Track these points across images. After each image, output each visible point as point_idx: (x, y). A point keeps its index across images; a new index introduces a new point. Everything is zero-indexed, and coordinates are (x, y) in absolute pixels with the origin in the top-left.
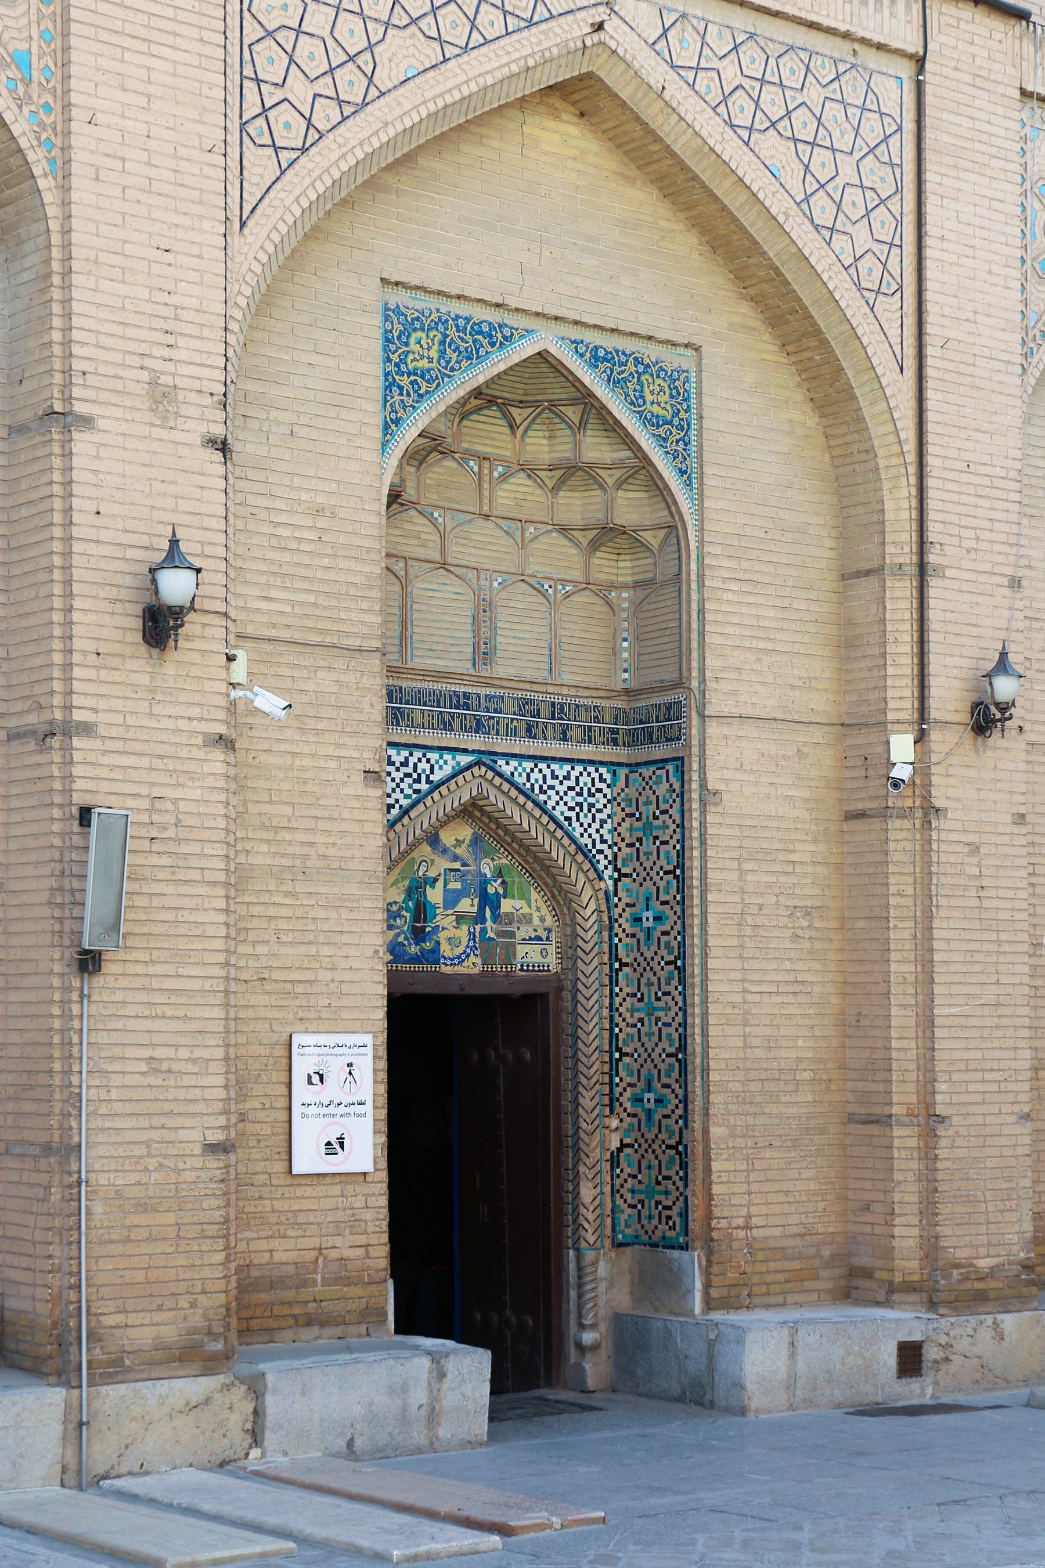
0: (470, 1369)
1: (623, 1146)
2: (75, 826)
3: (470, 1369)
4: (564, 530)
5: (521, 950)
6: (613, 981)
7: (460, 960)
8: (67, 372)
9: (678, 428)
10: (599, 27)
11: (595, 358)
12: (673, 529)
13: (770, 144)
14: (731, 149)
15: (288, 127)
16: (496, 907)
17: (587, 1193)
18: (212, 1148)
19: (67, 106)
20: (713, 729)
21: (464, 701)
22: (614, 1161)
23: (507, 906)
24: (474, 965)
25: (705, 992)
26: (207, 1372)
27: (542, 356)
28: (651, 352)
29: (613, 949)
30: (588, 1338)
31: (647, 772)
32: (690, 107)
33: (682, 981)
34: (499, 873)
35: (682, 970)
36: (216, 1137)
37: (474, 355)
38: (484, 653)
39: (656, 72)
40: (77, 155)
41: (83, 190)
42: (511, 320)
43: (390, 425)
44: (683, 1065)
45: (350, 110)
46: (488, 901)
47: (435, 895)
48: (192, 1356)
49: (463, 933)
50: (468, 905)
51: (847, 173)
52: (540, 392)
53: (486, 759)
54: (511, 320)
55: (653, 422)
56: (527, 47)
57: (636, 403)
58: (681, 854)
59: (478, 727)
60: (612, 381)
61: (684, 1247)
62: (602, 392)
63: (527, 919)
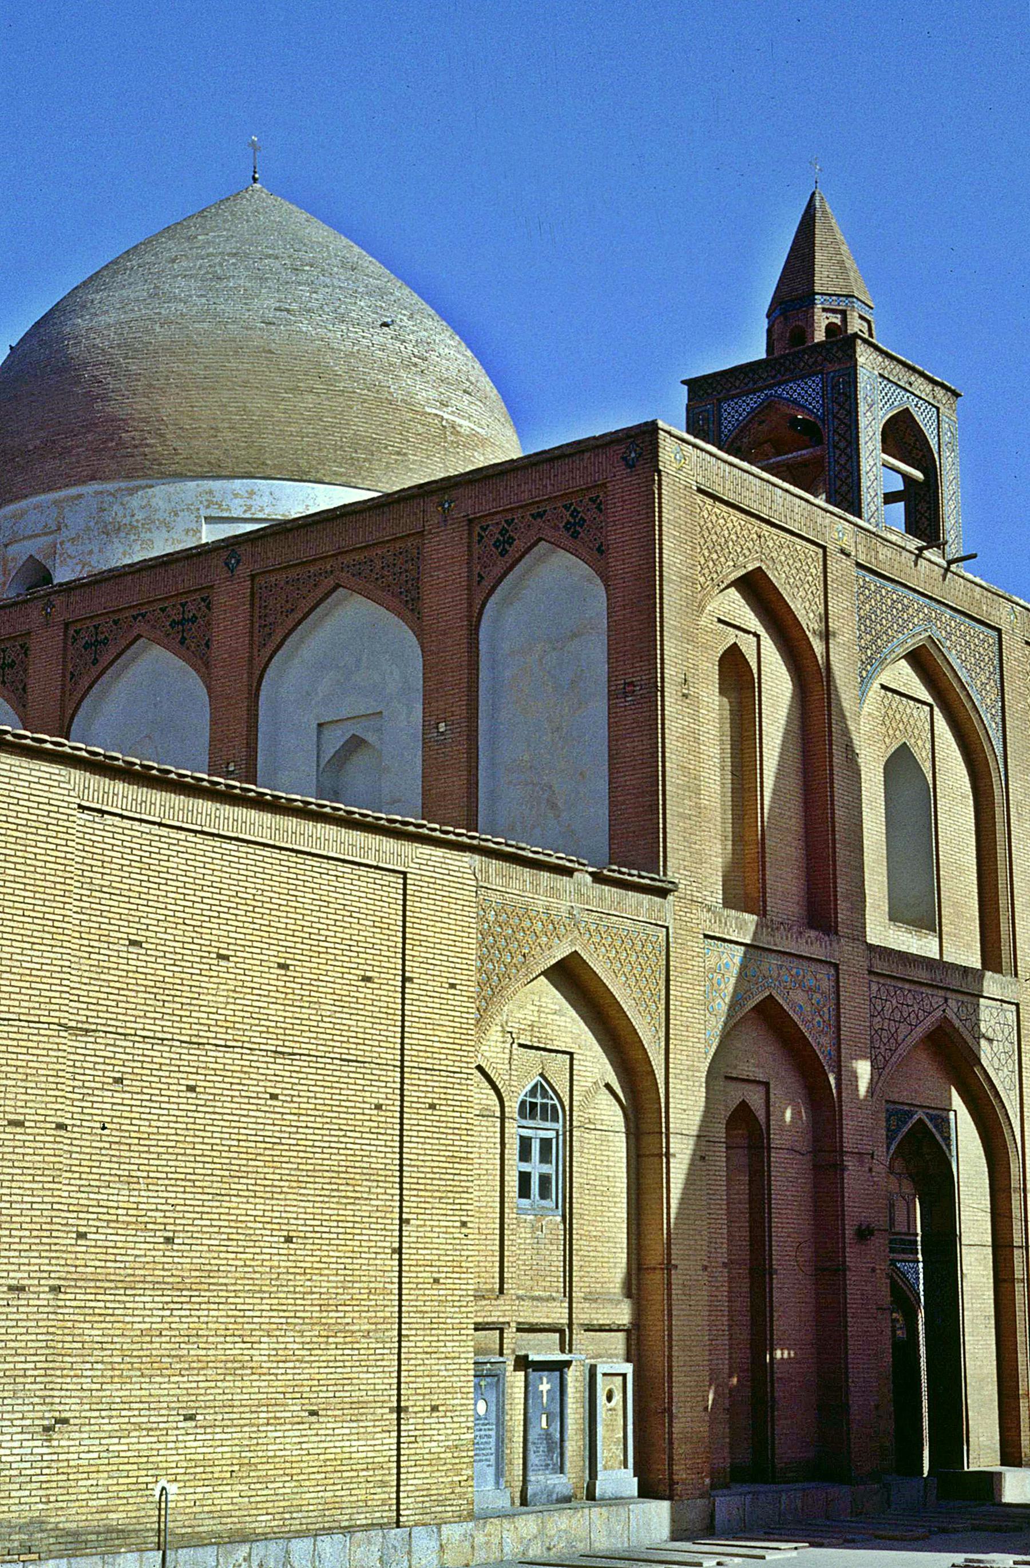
11: (932, 1118)
39: (957, 1023)
45: (893, 1051)
60: (935, 1127)
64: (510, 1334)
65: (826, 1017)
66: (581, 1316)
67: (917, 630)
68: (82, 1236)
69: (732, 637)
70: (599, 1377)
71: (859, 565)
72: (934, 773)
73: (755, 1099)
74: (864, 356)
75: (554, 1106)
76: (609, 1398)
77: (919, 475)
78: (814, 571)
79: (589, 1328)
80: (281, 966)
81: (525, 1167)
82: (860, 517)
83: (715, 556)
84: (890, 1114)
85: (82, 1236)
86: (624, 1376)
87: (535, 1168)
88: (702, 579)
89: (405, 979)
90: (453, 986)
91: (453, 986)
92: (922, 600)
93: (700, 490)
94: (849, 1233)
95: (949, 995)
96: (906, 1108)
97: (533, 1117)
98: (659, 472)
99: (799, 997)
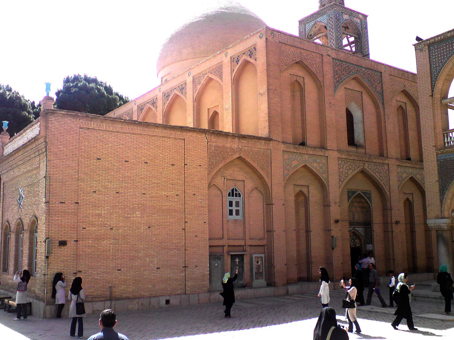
9: (369, 198)
11: (363, 193)
12: (369, 207)
13: (377, 174)
14: (374, 175)
21: (352, 223)
24: (353, 246)
37: (354, 194)
43: (348, 201)
45: (347, 177)
46: (354, 240)
52: (359, 196)
55: (367, 198)
57: (366, 196)
59: (353, 225)
60: (365, 195)
64: (226, 248)
66: (249, 242)
68: (85, 228)
70: (254, 257)
71: (333, 58)
73: (305, 190)
75: (239, 194)
76: (258, 262)
77: (357, 36)
79: (251, 246)
80: (145, 163)
81: (231, 208)
84: (349, 192)
85: (85, 228)
86: (262, 257)
87: (234, 208)
88: (282, 64)
89: (185, 164)
90: (200, 166)
91: (200, 166)
94: (332, 222)
97: (233, 196)
99: (315, 165)
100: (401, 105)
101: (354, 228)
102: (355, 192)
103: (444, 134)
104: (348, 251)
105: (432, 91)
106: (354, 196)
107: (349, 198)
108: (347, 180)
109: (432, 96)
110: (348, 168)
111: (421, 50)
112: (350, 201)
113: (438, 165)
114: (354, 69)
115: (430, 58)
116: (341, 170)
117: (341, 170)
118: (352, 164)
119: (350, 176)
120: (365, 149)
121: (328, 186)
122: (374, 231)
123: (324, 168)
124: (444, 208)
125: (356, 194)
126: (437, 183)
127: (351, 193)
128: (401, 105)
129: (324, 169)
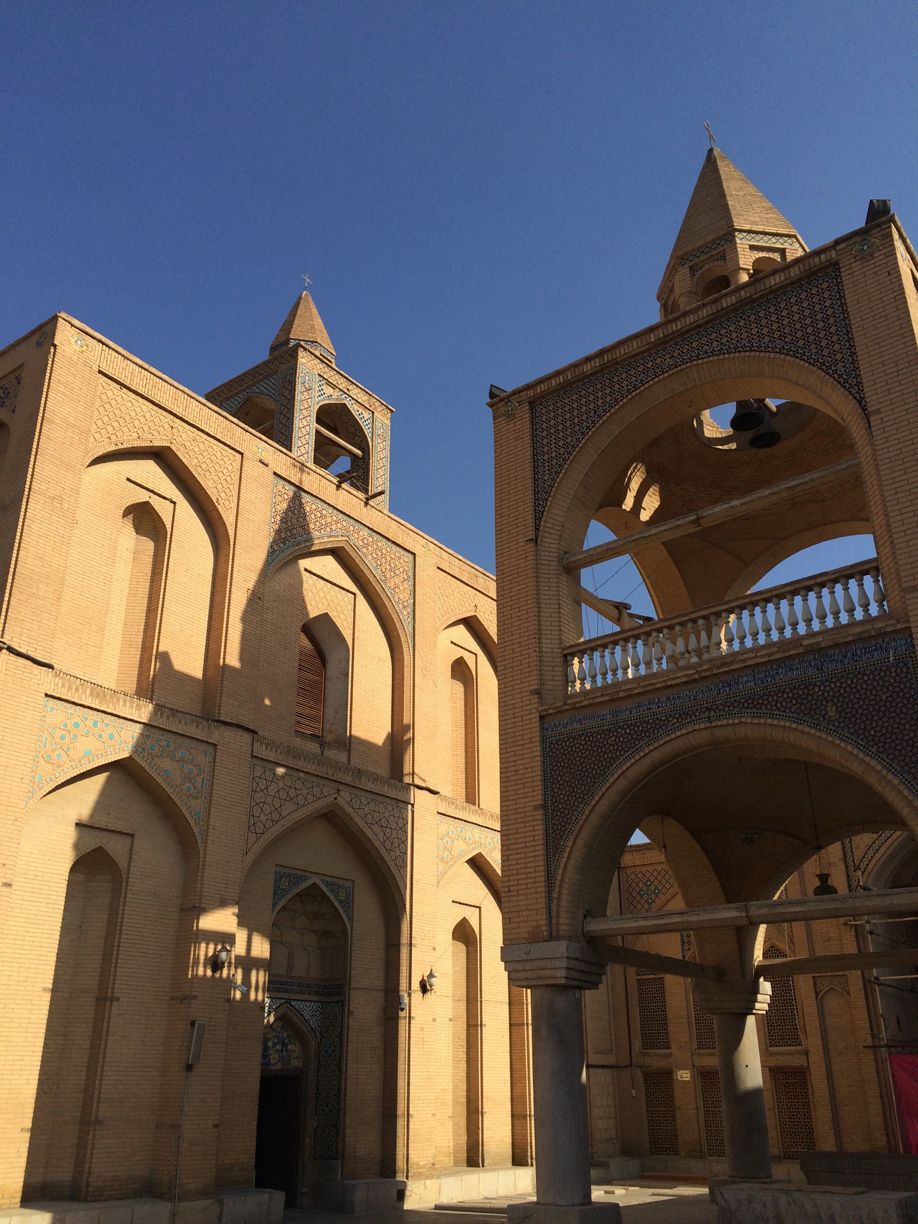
0: (279, 1197)
1: (318, 1125)
2: (189, 1026)
3: (279, 1197)
4: (313, 931)
5: (293, 1061)
6: (318, 1071)
7: (275, 1064)
8: (201, 895)
9: (348, 903)
10: (336, 799)
11: (327, 885)
12: (345, 932)
13: (376, 828)
14: (366, 830)
15: (259, 828)
16: (286, 1047)
17: (307, 1141)
18: (216, 1126)
19: (208, 825)
20: (352, 992)
21: (284, 983)
22: (315, 1130)
23: (289, 1047)
24: (279, 1066)
25: (346, 1075)
26: (209, 1198)
27: (314, 884)
28: (341, 882)
29: (319, 1061)
30: (305, 1190)
31: (332, 1005)
32: (357, 820)
33: (340, 1071)
34: (288, 1037)
35: (340, 1068)
36: (217, 1122)
37: (297, 884)
38: (290, 968)
39: (348, 810)
40: (210, 838)
41: (210, 847)
42: (307, 874)
44: (339, 1099)
46: (285, 1045)
47: (270, 1044)
48: (204, 1193)
49: (277, 1056)
50: (279, 1047)
51: (394, 835)
52: (313, 894)
53: (288, 1001)
54: (307, 874)
55: (341, 902)
56: (318, 804)
57: (337, 896)
58: (341, 1031)
59: (287, 992)
60: (332, 891)
61: (336, 1159)
62: (328, 893)
63: (295, 1051)
65: (199, 784)
67: (334, 533)
69: (144, 496)
71: (275, 474)
72: (353, 639)
74: (304, 360)
77: (358, 452)
78: (230, 467)
82: (291, 451)
83: (115, 424)
84: (278, 877)
92: (341, 516)
93: (100, 372)
95: (341, 787)
96: (299, 873)
98: (55, 346)
99: (167, 764)
100: (462, 658)
101: (288, 1001)
102: (303, 879)
103: (565, 656)
104: (253, 1085)
105: (537, 529)
106: (297, 890)
107: (278, 892)
108: (277, 829)
109: (535, 541)
110: (283, 795)
111: (510, 416)
112: (279, 907)
113: (544, 756)
114: (337, 522)
115: (534, 436)
116: (259, 797)
117: (259, 797)
118: (299, 785)
119: (287, 822)
120: (349, 751)
121: (205, 843)
122: (350, 1013)
123: (199, 779)
124: (559, 898)
125: (303, 886)
126: (539, 814)
127: (285, 878)
128: (462, 658)
129: (199, 784)
